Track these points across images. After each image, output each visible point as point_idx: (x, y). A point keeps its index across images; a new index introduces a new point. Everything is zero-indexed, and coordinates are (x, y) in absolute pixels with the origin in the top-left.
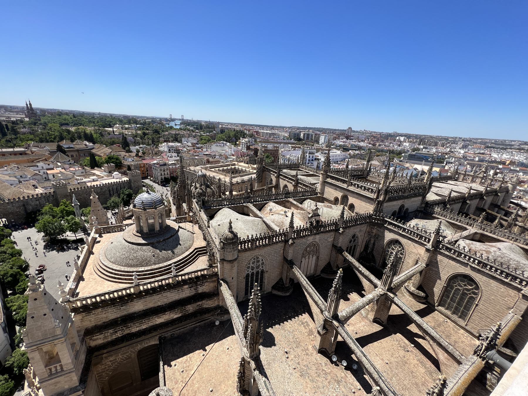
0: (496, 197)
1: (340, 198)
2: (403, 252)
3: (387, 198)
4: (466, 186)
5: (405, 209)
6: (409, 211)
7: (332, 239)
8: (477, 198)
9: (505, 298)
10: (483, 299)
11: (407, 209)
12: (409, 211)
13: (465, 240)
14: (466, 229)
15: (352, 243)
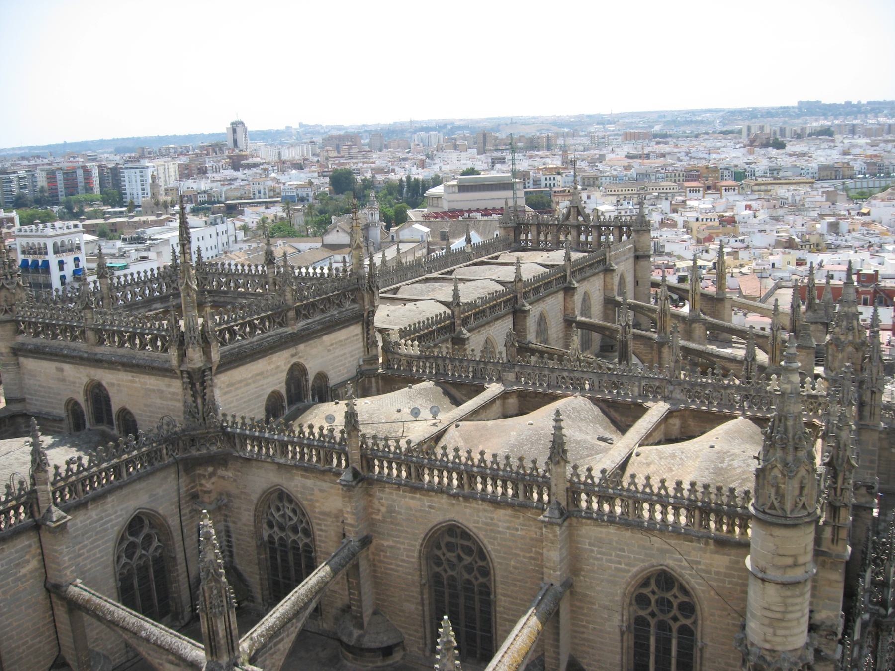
0: (609, 276)
1: (80, 398)
2: (308, 523)
3: (215, 356)
4: (540, 261)
5: (311, 377)
6: (334, 380)
7: (34, 564)
8: (557, 292)
9: (531, 551)
10: (498, 579)
11: (322, 377)
12: (334, 380)
13: (460, 423)
14: (480, 389)
15: (139, 552)
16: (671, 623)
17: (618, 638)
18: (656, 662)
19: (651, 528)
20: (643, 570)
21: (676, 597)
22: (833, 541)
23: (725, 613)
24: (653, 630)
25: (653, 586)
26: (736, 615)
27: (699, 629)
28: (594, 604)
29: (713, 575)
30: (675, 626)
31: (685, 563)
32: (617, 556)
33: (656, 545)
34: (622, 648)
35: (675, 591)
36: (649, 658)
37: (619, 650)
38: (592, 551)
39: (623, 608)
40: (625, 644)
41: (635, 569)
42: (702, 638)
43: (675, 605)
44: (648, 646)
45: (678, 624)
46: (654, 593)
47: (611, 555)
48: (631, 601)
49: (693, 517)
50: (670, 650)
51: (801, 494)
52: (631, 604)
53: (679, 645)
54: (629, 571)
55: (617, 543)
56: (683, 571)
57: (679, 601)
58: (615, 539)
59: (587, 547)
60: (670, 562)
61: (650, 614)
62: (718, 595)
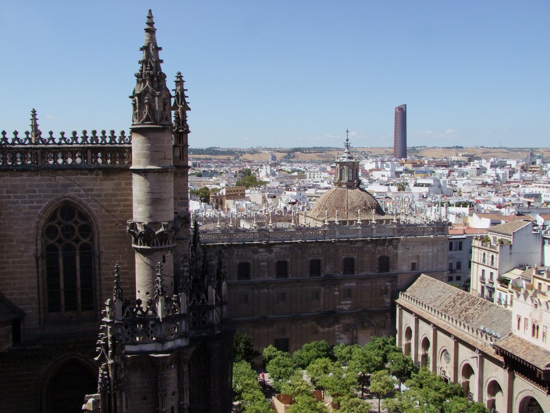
16: (74, 244)
17: (34, 264)
18: (65, 280)
19: (56, 169)
20: (51, 203)
21: (76, 223)
22: (180, 156)
23: (114, 225)
24: (60, 253)
25: (59, 217)
26: (121, 224)
27: (96, 242)
28: (13, 241)
29: (103, 198)
30: (77, 247)
31: (82, 192)
32: (30, 197)
33: (60, 182)
34: (38, 273)
35: (76, 218)
36: (59, 277)
37: (35, 275)
38: (9, 197)
39: (37, 239)
40: (40, 269)
41: (44, 205)
42: (99, 249)
43: (77, 229)
44: (58, 268)
45: (80, 243)
46: (59, 223)
47: (25, 197)
48: (42, 233)
49: (86, 158)
50: (75, 267)
51: (164, 110)
52: (42, 236)
53: (81, 261)
54: (40, 207)
55: (29, 186)
56: (82, 199)
57: (79, 225)
58: (28, 183)
59: (5, 194)
60: (72, 194)
61: (57, 241)
62: (108, 211)
